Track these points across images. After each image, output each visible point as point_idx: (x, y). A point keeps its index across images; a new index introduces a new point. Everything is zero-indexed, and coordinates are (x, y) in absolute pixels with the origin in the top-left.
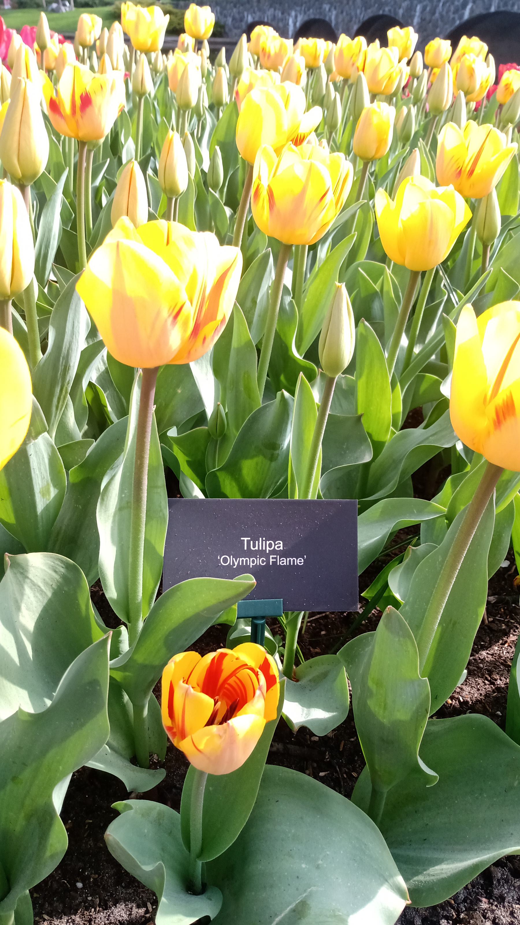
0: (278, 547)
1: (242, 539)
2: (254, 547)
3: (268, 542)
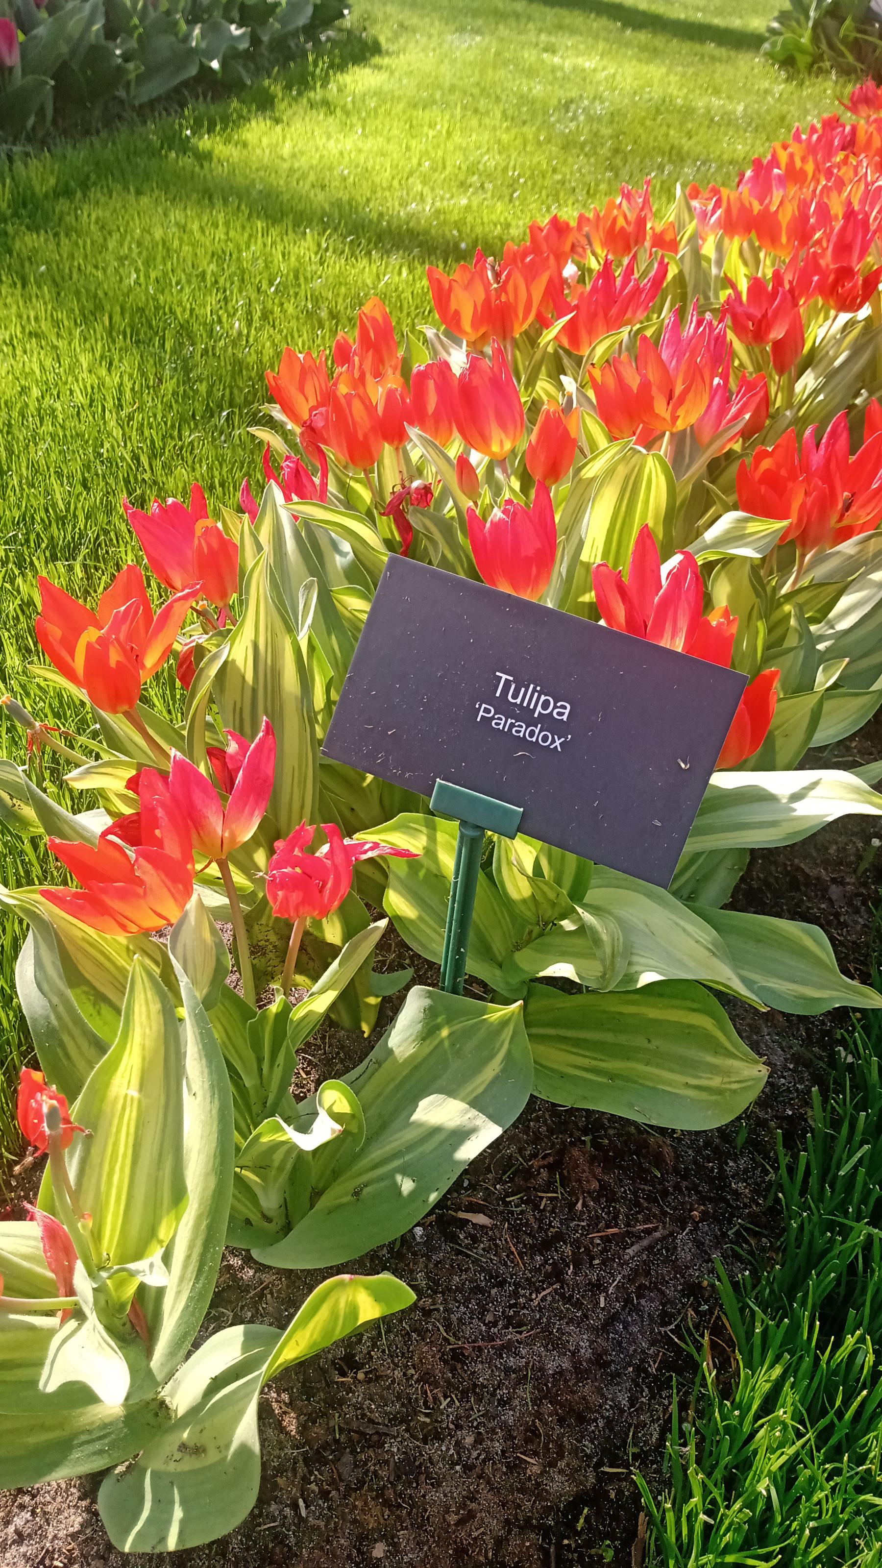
0: (559, 714)
2: (515, 697)
3: (543, 698)
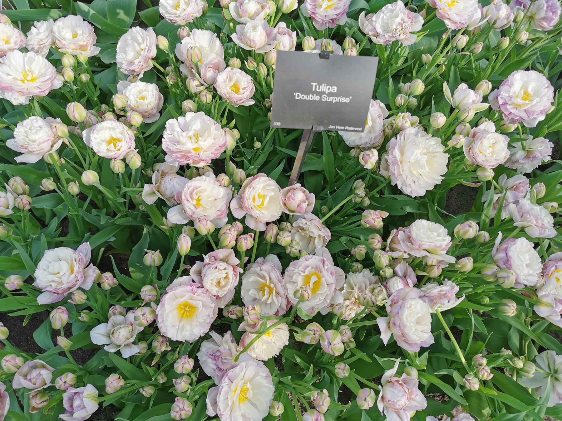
1: (312, 84)
2: (319, 89)
